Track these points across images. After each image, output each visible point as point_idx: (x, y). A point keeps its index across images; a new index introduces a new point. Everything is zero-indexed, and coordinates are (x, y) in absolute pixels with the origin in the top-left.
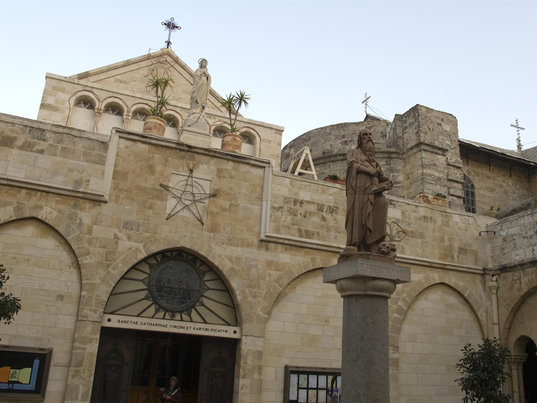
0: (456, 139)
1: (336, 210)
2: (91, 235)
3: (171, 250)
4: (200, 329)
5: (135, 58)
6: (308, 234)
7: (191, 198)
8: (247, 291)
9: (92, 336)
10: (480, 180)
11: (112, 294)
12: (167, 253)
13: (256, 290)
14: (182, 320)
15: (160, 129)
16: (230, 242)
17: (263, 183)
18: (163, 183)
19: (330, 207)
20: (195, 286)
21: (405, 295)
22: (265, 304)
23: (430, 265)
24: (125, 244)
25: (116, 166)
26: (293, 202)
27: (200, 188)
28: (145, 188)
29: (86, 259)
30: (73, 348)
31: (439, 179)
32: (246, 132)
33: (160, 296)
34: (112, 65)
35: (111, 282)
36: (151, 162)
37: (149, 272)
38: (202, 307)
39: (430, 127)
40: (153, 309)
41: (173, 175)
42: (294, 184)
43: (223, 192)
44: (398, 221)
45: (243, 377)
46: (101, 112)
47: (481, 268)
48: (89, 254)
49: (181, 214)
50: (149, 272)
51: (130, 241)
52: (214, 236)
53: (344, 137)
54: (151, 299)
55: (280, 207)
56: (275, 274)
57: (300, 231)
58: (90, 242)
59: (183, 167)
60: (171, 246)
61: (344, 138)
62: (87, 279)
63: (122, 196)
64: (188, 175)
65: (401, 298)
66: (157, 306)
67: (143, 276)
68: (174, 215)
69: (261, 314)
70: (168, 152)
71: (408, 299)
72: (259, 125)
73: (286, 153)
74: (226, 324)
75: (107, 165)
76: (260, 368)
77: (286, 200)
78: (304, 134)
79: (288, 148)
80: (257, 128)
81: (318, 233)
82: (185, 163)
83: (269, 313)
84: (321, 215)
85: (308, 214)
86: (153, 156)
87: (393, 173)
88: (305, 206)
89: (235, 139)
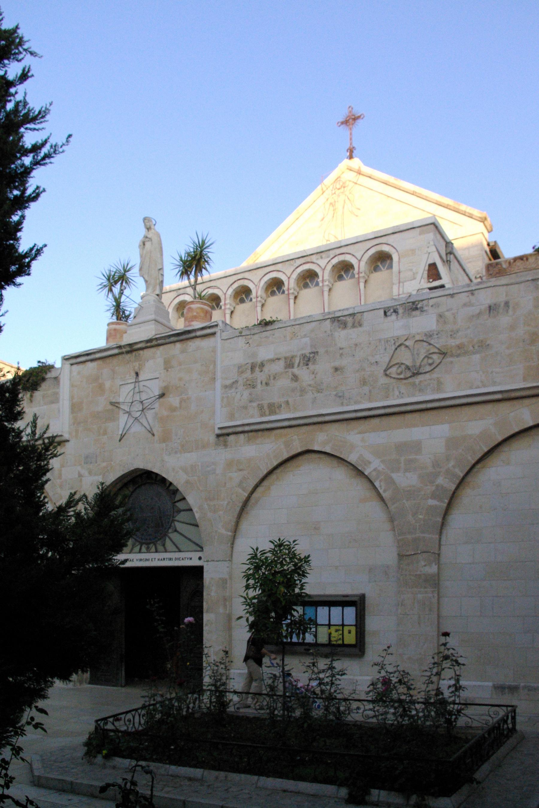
1: (314, 357)
2: (61, 479)
6: (273, 408)
16: (184, 448)
18: (114, 401)
19: (304, 356)
21: (452, 463)
23: (506, 395)
26: (250, 368)
36: (100, 381)
42: (250, 341)
49: (133, 430)
51: (91, 476)
52: (167, 446)
55: (233, 383)
56: (236, 476)
57: (261, 407)
58: (61, 486)
59: (130, 373)
64: (134, 381)
68: (125, 434)
70: (115, 360)
72: (393, 233)
77: (240, 370)
80: (390, 239)
81: (287, 403)
84: (290, 374)
85: (272, 378)
88: (266, 369)
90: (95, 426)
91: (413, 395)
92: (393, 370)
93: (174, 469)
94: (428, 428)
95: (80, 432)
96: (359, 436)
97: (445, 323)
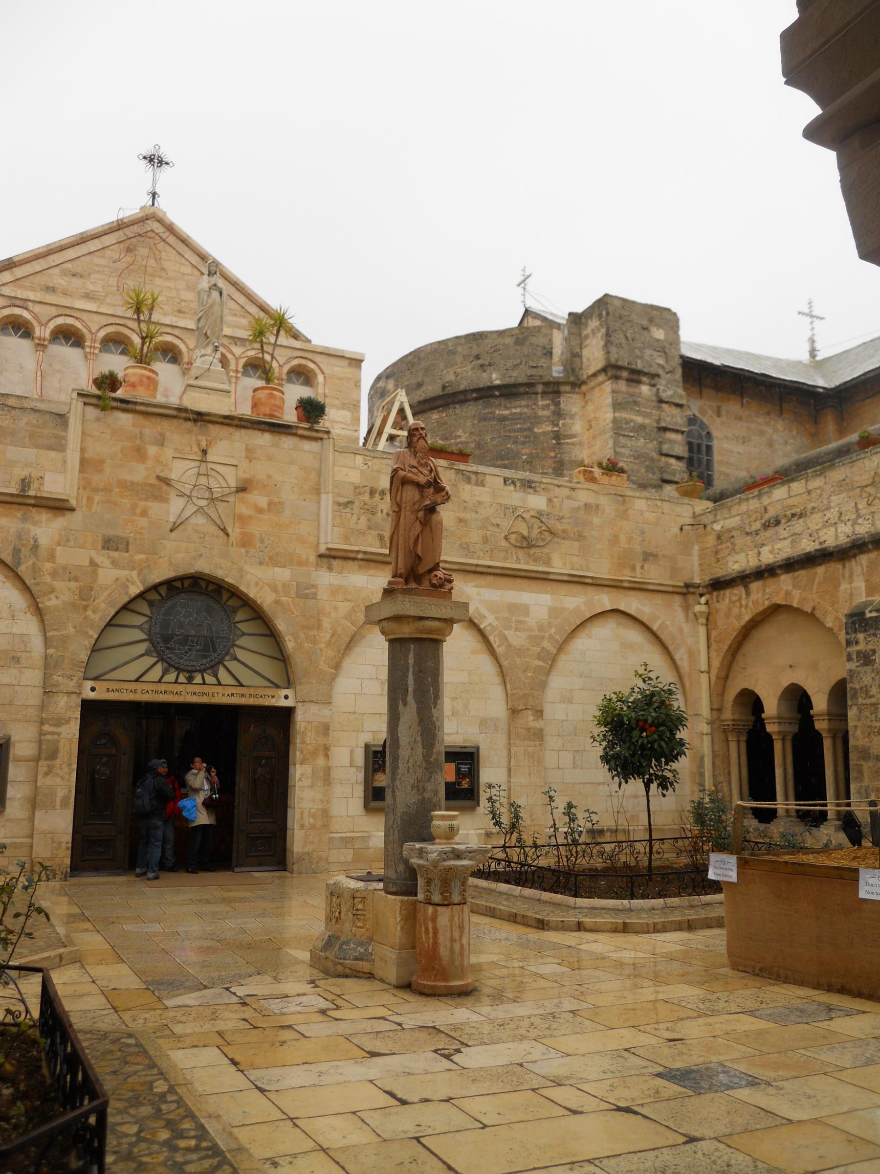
0: (676, 353)
3: (182, 579)
4: (233, 695)
5: (95, 229)
7: (207, 495)
8: (302, 635)
9: (69, 714)
10: (723, 423)
11: (94, 650)
12: (174, 583)
13: (315, 632)
14: (204, 683)
15: (149, 386)
17: (321, 465)
18: (162, 475)
20: (223, 630)
21: (553, 630)
22: (330, 653)
24: (107, 575)
25: (83, 450)
26: (368, 492)
27: (220, 478)
28: (132, 483)
29: (50, 599)
30: (41, 733)
31: (642, 427)
32: (300, 366)
33: (168, 648)
34: (54, 243)
35: (91, 633)
36: (138, 442)
37: (148, 613)
38: (235, 662)
39: (628, 335)
40: (158, 670)
41: (175, 460)
42: (370, 463)
43: (257, 483)
44: (542, 515)
45: (301, 764)
46: (46, 343)
47: (682, 584)
48: (53, 590)
49: (193, 520)
50: (148, 613)
52: (247, 552)
53: (477, 357)
54: (155, 655)
55: (349, 502)
56: (344, 608)
60: (181, 572)
61: (479, 359)
62: (54, 630)
63: (97, 498)
64: (199, 458)
65: (547, 635)
66: (165, 665)
67: (140, 620)
68: (181, 523)
69: (327, 669)
71: (557, 637)
73: (381, 388)
74: (271, 685)
75: (69, 451)
76: (327, 749)
77: (357, 491)
78: (411, 353)
79: (384, 379)
80: (318, 359)
82: (194, 438)
83: (337, 667)
86: (141, 432)
87: (565, 419)
89: (272, 394)
90: (125, 501)
91: (528, 563)
92: (513, 536)
93: (257, 584)
94: (534, 595)
95: (95, 503)
96: (476, 590)
97: (553, 506)
